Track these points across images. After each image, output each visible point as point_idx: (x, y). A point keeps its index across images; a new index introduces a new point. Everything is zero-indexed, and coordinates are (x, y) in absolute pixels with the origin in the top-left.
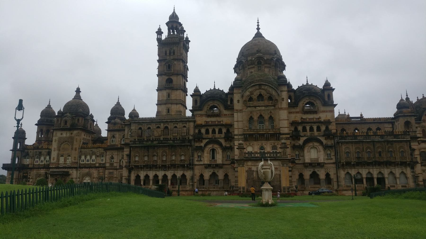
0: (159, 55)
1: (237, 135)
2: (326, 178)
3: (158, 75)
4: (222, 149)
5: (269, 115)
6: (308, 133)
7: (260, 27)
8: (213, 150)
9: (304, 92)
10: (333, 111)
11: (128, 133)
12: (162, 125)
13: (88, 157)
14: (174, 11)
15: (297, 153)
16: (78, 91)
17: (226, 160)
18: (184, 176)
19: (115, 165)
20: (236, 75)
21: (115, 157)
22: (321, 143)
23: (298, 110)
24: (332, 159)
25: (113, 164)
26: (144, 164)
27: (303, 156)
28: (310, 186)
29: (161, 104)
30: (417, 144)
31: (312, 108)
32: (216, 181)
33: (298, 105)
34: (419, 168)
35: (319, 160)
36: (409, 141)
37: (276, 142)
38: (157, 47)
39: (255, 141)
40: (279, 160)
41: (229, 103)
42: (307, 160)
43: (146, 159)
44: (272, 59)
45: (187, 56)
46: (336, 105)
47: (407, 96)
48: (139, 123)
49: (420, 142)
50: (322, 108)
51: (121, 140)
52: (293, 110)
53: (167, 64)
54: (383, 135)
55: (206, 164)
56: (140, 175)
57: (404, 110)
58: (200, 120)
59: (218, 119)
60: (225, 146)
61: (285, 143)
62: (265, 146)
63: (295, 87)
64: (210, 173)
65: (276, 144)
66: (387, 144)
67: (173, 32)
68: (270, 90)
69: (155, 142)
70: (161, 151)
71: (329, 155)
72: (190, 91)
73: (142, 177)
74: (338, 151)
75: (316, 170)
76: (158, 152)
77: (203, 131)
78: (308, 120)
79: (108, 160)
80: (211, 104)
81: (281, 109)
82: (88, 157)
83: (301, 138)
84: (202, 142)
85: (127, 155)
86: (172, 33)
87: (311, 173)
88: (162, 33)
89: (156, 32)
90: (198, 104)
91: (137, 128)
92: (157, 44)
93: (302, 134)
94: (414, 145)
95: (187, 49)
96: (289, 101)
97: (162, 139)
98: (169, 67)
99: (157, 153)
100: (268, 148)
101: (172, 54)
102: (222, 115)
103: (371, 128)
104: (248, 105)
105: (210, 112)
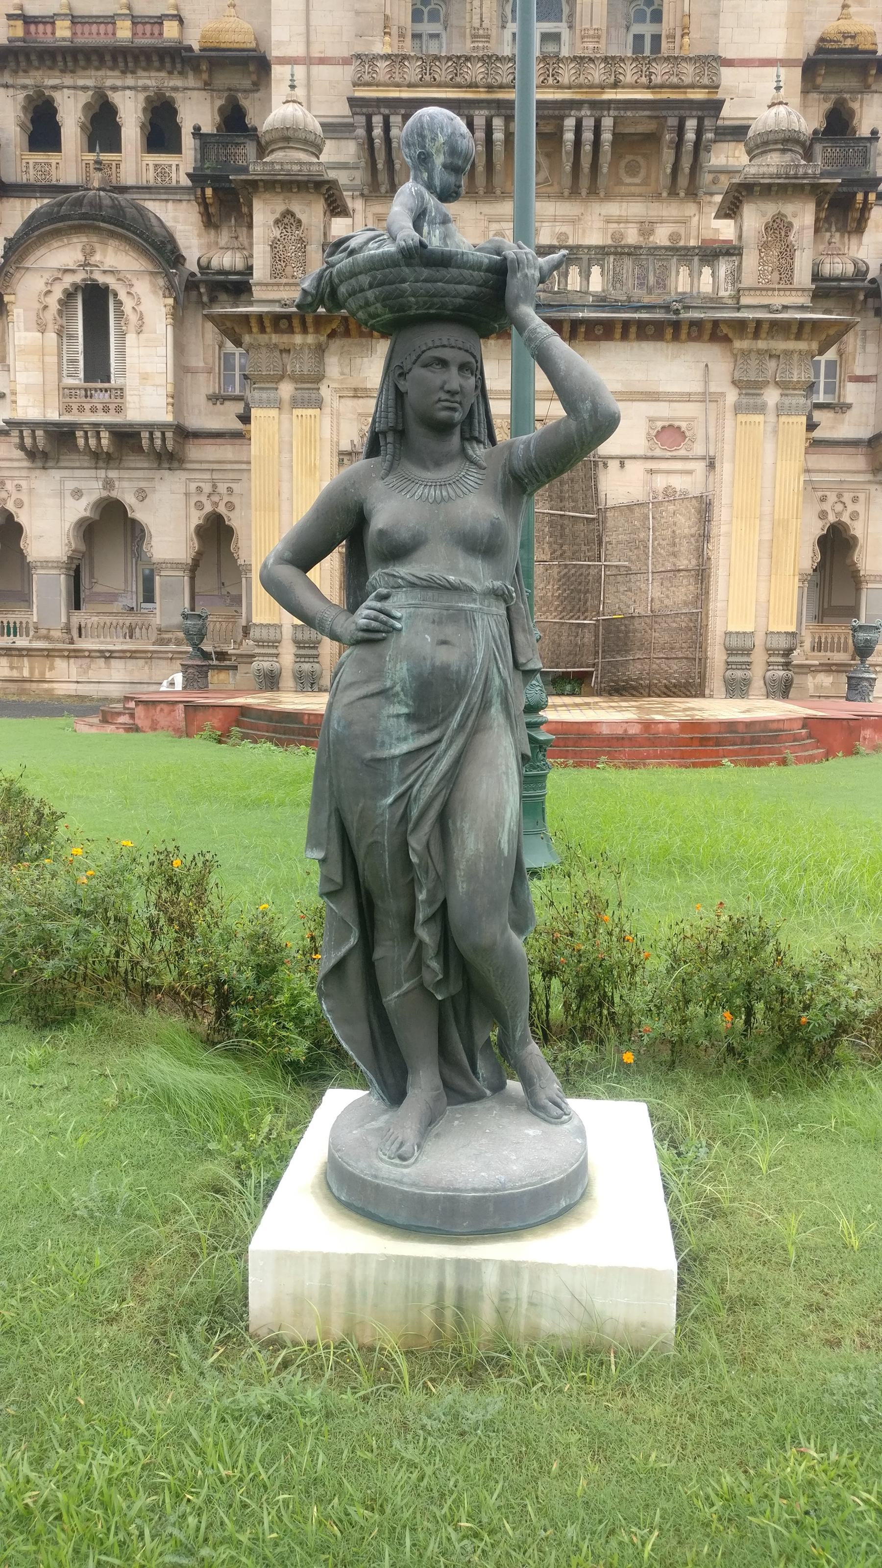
4: (170, 288)
8: (95, 303)
17: (216, 399)
37: (671, 210)
40: (716, 332)
55: (33, 425)
60: (204, 268)
64: (80, 509)
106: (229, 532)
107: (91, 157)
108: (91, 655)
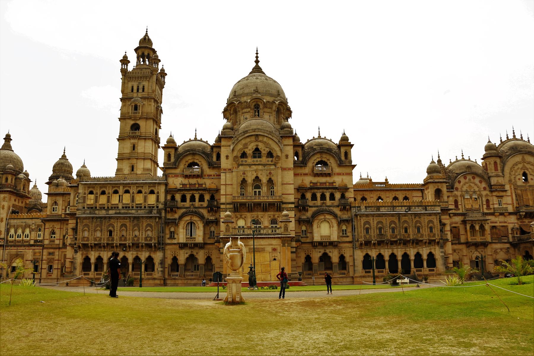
0: (123, 92)
1: (223, 204)
2: (340, 261)
3: (120, 119)
4: (203, 222)
5: (269, 177)
6: (319, 202)
7: (259, 59)
8: (191, 223)
9: (314, 147)
10: (351, 174)
11: (74, 198)
12: (121, 187)
13: (20, 231)
14: (147, 33)
15: (304, 228)
16: (8, 138)
17: (209, 238)
18: (150, 259)
19: (57, 242)
20: (224, 122)
21: (57, 231)
22: (335, 216)
23: (307, 170)
24: (348, 237)
25: (54, 241)
26: (96, 242)
27: (312, 233)
28: (319, 273)
29: (122, 159)
30: (448, 217)
31: (325, 169)
32: (195, 266)
33: (306, 164)
34: (449, 247)
35: (332, 238)
36: (439, 213)
38: (121, 81)
39: (249, 211)
41: (215, 159)
42: (317, 238)
43: (98, 234)
44: (274, 102)
45: (162, 94)
46: (355, 166)
47: (439, 157)
48: (89, 186)
49: (451, 215)
50: (337, 170)
51: (66, 207)
52: (300, 171)
53: (133, 105)
54: (411, 206)
55: (182, 243)
56: (90, 256)
57: (435, 175)
58: (176, 182)
59: (201, 181)
61: (287, 216)
62: (262, 219)
63: (303, 141)
64: (187, 256)
65: (276, 216)
66: (415, 217)
67: (144, 61)
68: (271, 142)
69: (111, 212)
70: (119, 224)
71: (344, 232)
72: (163, 142)
73: (93, 260)
74: (356, 227)
75: (327, 251)
76: (115, 225)
77: (178, 197)
78: (318, 184)
79: (47, 236)
80: (190, 159)
81: (283, 169)
82: (20, 231)
83: (309, 209)
84: (175, 212)
85: (73, 229)
86: (142, 63)
87: (320, 254)
88: (129, 62)
89: (121, 61)
90: (173, 159)
91: (87, 192)
92: (121, 77)
93: (311, 203)
94: (446, 219)
95: (161, 85)
96: (296, 158)
97: (120, 207)
98: (136, 108)
99: (113, 227)
100: (266, 222)
101: (141, 90)
102: (205, 176)
103: (397, 196)
104: (241, 163)
105: (188, 172)
106: (211, 259)
107: (191, 203)
108: (188, 279)
